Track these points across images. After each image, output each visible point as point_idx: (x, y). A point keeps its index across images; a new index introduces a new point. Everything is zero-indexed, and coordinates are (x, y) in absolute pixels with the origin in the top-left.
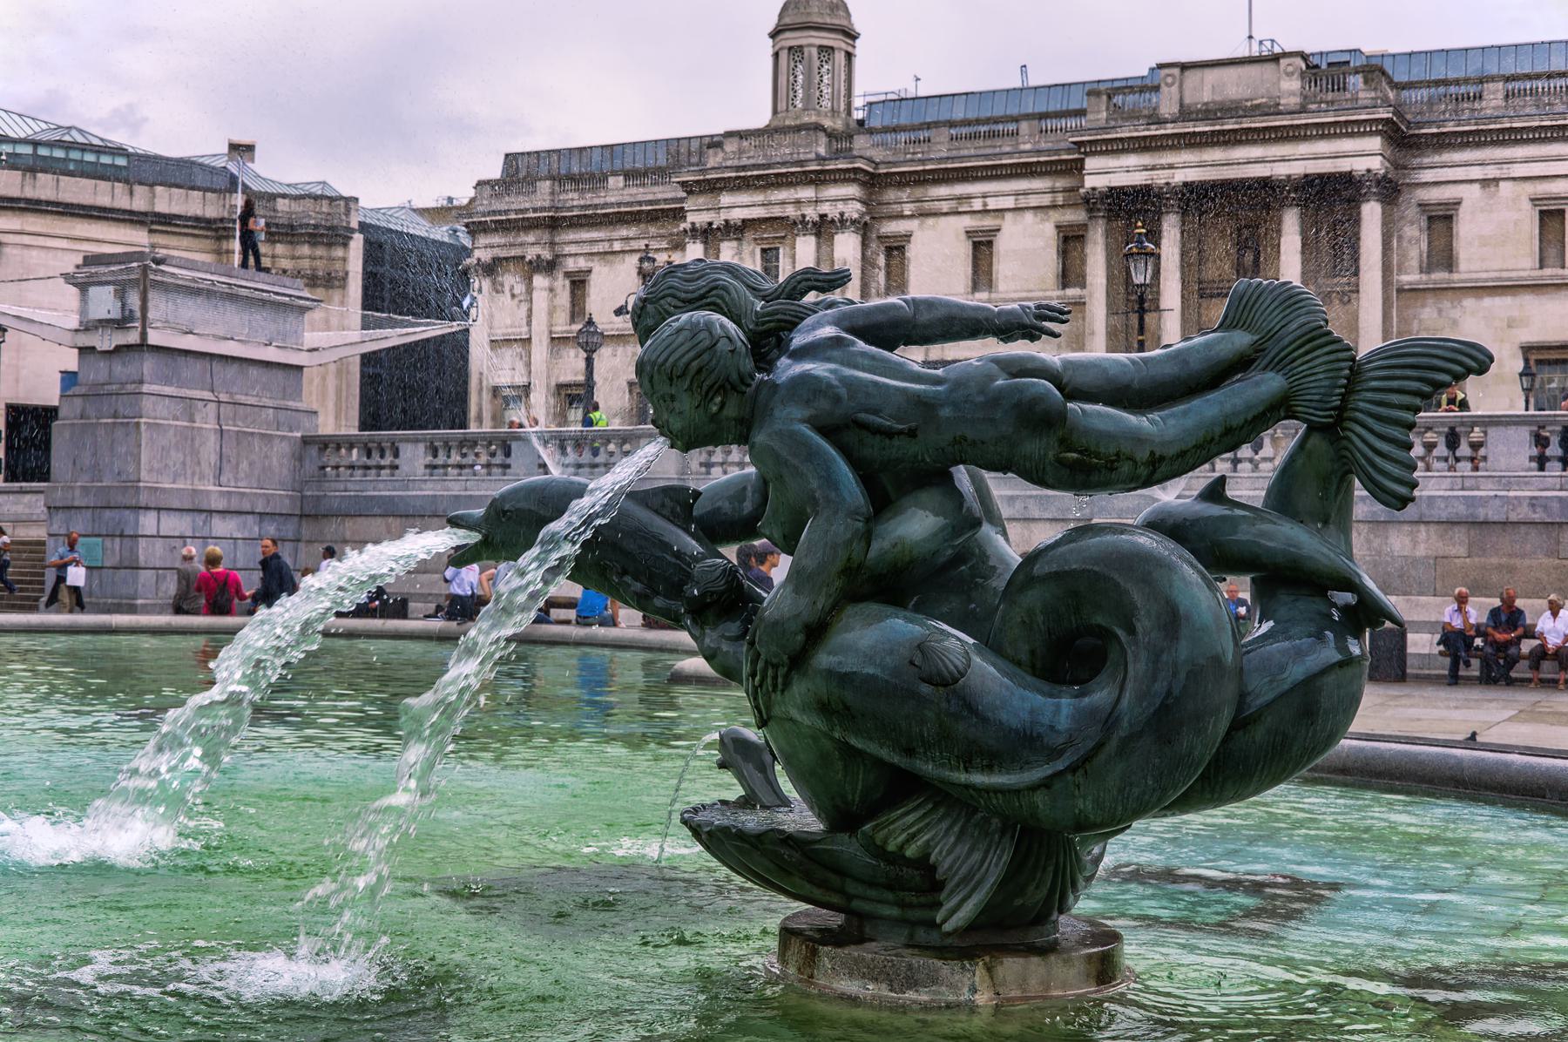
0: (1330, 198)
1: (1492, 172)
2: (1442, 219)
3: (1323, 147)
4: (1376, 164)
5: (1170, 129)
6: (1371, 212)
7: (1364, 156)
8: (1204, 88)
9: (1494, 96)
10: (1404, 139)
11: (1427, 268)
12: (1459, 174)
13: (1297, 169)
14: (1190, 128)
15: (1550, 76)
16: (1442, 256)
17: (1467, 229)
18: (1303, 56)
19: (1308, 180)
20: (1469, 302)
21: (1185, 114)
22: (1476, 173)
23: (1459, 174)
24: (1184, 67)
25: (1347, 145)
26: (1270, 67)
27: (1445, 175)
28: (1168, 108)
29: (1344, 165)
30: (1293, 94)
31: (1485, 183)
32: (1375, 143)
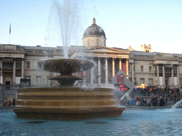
0: (19, 60)
1: (34, 59)
2: (28, 63)
3: (18, 55)
4: (24, 57)
5: (2, 51)
6: (23, 62)
7: (22, 56)
8: (6, 47)
9: (34, 51)
10: (26, 55)
11: (27, 68)
12: (31, 59)
13: (16, 57)
14: (4, 51)
15: (39, 50)
16: (28, 67)
17: (31, 64)
18: (16, 45)
19: (17, 58)
20: (31, 71)
21: (4, 50)
22: (32, 59)
23: (31, 59)
24: (4, 45)
25: (21, 55)
26: (13, 46)
27: (29, 59)
28: (2, 49)
29: (20, 57)
30: (15, 49)
31: (33, 60)
32: (24, 55)
